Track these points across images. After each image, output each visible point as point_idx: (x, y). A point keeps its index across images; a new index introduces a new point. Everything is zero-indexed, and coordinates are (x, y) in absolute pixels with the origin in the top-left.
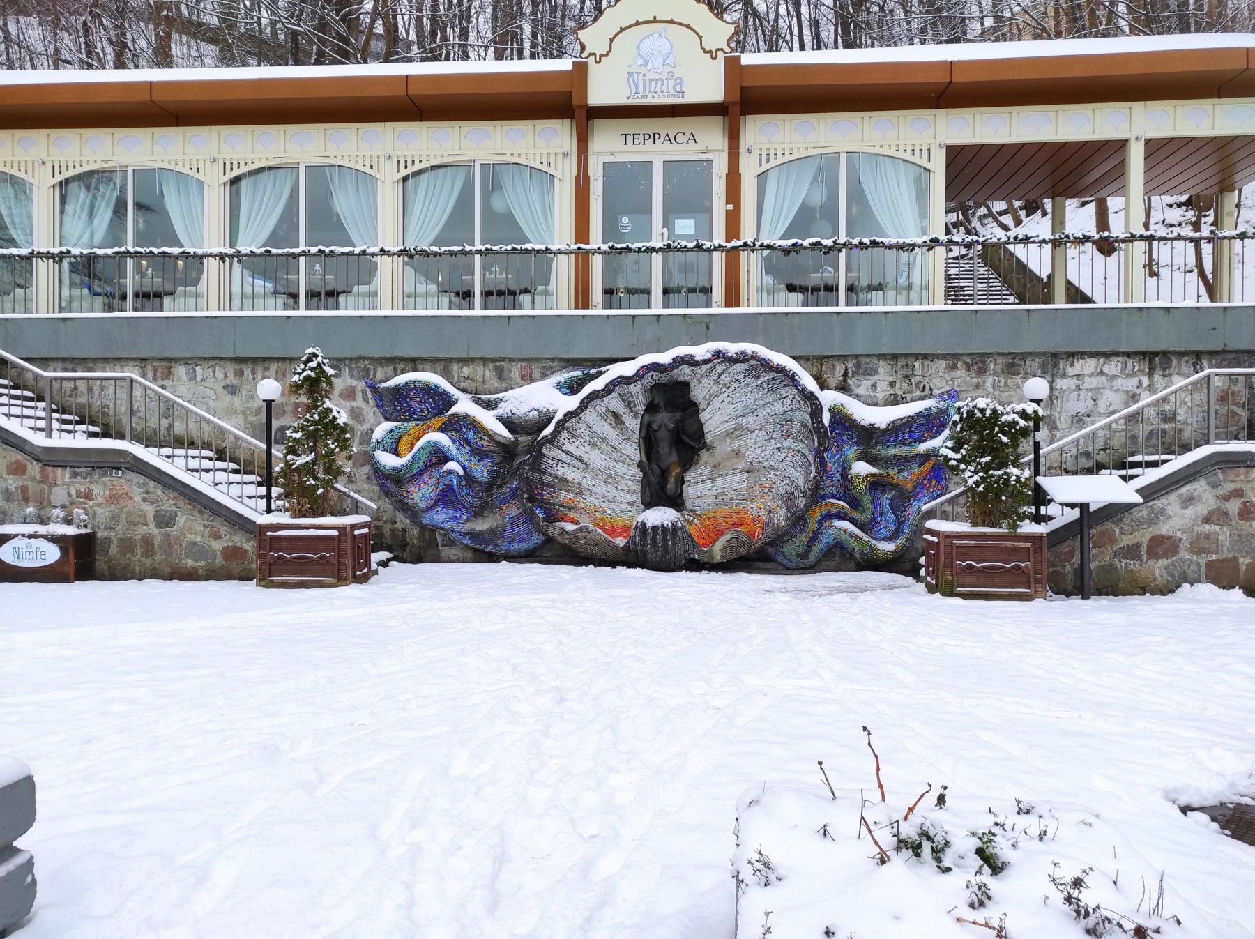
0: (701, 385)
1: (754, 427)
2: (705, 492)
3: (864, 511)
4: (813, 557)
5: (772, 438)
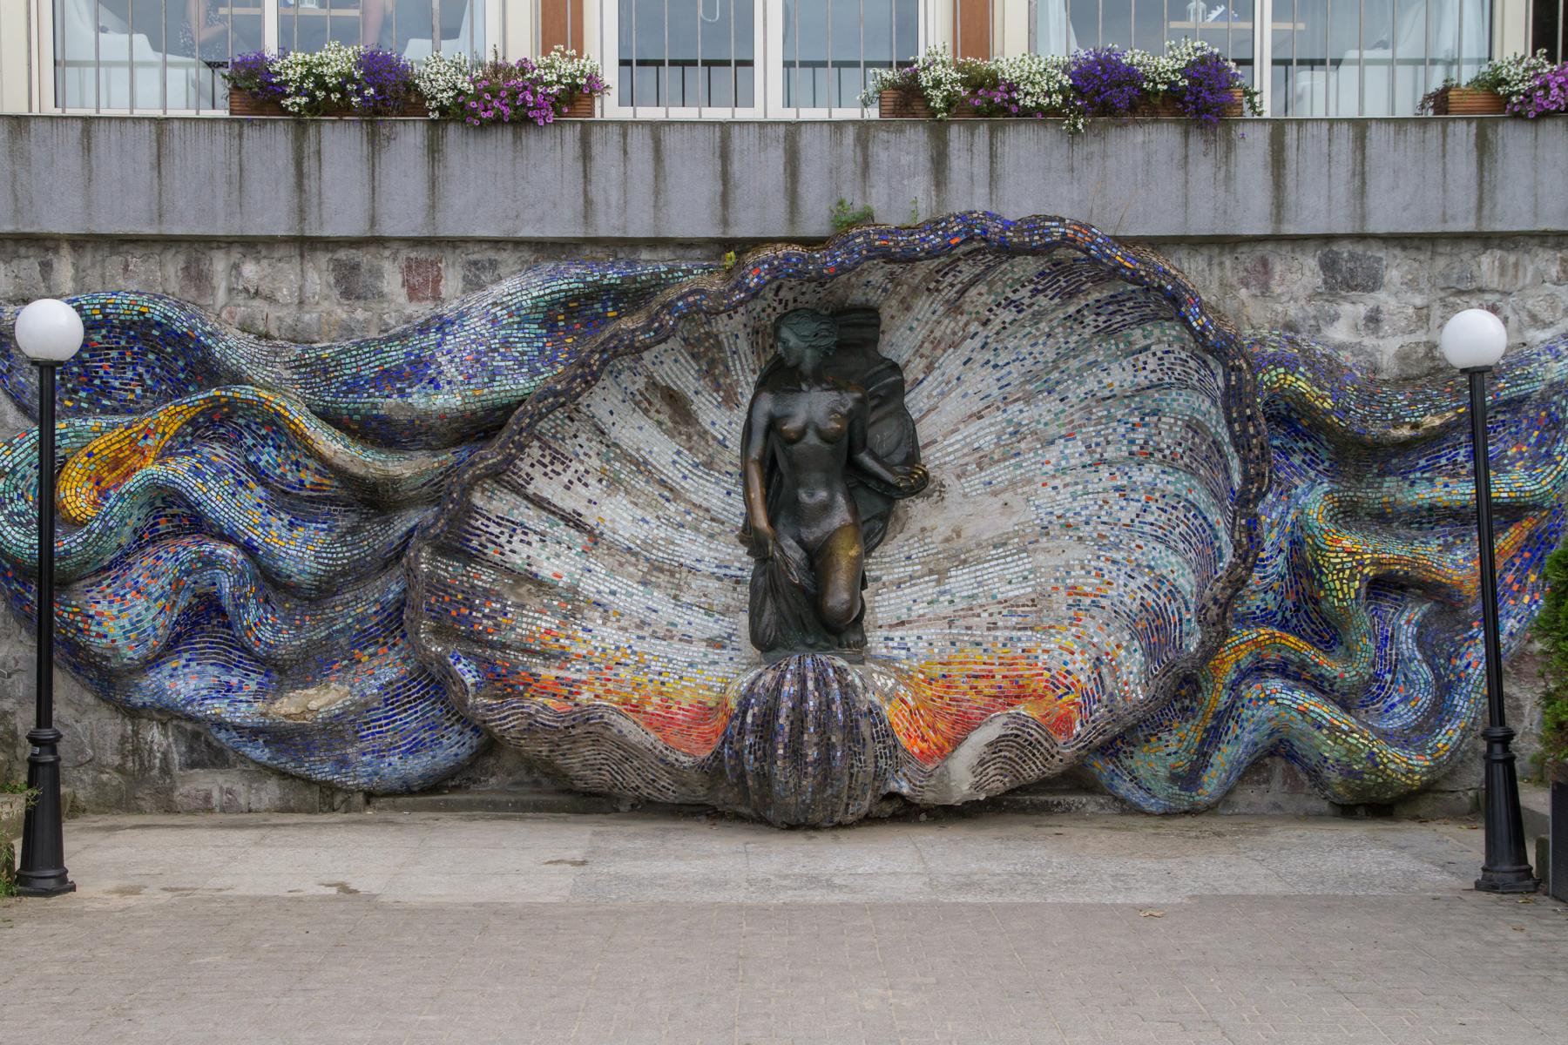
0: (910, 315)
1: (1053, 430)
2: (919, 609)
3: (1350, 656)
4: (1211, 783)
5: (1102, 461)
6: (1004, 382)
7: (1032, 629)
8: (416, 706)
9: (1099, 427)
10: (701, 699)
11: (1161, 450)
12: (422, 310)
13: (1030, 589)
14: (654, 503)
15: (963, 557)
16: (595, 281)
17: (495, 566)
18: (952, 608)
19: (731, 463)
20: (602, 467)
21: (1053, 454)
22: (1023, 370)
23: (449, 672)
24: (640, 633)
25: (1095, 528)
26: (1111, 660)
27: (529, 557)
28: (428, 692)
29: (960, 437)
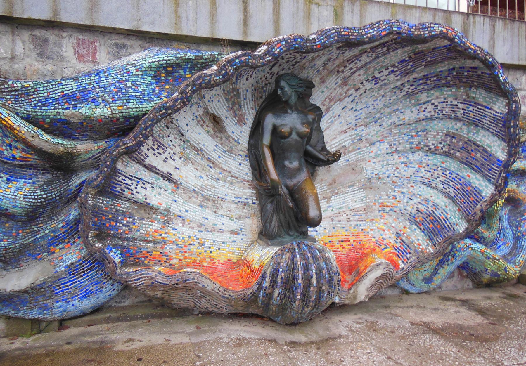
0: (323, 85)
1: (375, 139)
5: (396, 151)
6: (358, 118)
7: (365, 221)
8: (87, 273)
9: (395, 137)
10: (229, 258)
11: (427, 146)
12: (86, 68)
13: (364, 204)
14: (205, 169)
15: (336, 191)
16: (181, 57)
17: (128, 200)
18: (332, 213)
19: (241, 150)
20: (181, 152)
21: (374, 149)
22: (367, 112)
23: (106, 257)
24: (200, 229)
25: (391, 179)
26: (404, 233)
27: (145, 195)
28: (94, 266)
29: (337, 141)
